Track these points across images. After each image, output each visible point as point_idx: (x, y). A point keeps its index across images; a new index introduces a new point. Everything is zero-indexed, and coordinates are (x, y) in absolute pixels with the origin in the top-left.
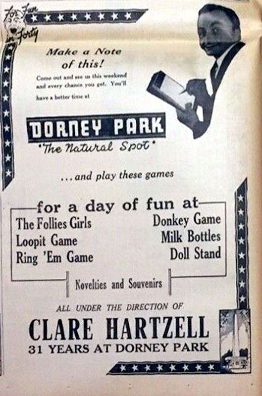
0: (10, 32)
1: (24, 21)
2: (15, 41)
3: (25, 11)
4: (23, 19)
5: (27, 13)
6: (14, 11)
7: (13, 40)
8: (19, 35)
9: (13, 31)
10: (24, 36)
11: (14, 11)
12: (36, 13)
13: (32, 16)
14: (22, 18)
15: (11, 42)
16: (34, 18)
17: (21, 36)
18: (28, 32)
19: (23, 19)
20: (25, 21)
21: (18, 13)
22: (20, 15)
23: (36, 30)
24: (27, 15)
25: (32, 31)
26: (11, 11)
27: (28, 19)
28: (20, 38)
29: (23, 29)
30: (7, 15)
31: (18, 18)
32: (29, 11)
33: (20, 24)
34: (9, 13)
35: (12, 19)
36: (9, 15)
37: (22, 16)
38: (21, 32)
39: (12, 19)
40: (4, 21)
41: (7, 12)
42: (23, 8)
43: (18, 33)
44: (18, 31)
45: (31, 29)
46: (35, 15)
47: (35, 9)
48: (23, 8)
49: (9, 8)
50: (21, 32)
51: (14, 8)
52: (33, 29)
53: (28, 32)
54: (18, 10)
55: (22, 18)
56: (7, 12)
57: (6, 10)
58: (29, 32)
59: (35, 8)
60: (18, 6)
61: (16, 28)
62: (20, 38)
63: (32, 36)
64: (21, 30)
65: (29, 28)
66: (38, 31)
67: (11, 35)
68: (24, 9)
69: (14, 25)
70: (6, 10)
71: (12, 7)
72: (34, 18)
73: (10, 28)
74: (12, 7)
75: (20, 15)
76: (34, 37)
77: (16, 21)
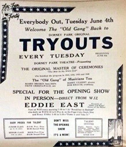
0: (4, 15)
1: (12, 11)
2: (7, 19)
3: (12, 6)
4: (11, 10)
5: (14, 7)
6: (7, 6)
7: (6, 19)
8: (9, 17)
9: (6, 15)
10: (11, 17)
11: (7, 6)
12: (18, 7)
13: (16, 8)
14: (11, 9)
15: (5, 20)
16: (17, 9)
17: (11, 17)
18: (14, 16)
19: (11, 10)
20: (13, 11)
21: (9, 6)
22: (10, 7)
23: (18, 15)
24: (14, 8)
25: (16, 15)
26: (5, 6)
27: (14, 10)
28: (10, 18)
29: (11, 14)
30: (3, 8)
31: (9, 9)
32: (15, 6)
33: (10, 12)
34: (4, 7)
35: (6, 9)
36: (4, 8)
37: (11, 8)
38: (10, 15)
39: (6, 9)
40: (2, 10)
41: (3, 6)
42: (11, 4)
43: (9, 16)
44: (9, 15)
45: (16, 14)
46: (18, 8)
47: (18, 5)
48: (11, 4)
49: (4, 4)
50: (10, 15)
51: (7, 5)
52: (17, 14)
53: (14, 16)
54: (9, 5)
55: (11, 9)
56: (3, 6)
57: (3, 5)
58: (15, 15)
59: (18, 5)
60: (9, 3)
61: (8, 13)
62: (10, 18)
63: (16, 17)
64: (10, 14)
65: (15, 14)
66: (19, 15)
67: (5, 16)
68: (12, 5)
69: (7, 12)
70: (3, 5)
71: (6, 4)
72: (17, 9)
73: (5, 13)
74: (6, 4)
75: (10, 7)
76: (17, 18)
77: (8, 11)
